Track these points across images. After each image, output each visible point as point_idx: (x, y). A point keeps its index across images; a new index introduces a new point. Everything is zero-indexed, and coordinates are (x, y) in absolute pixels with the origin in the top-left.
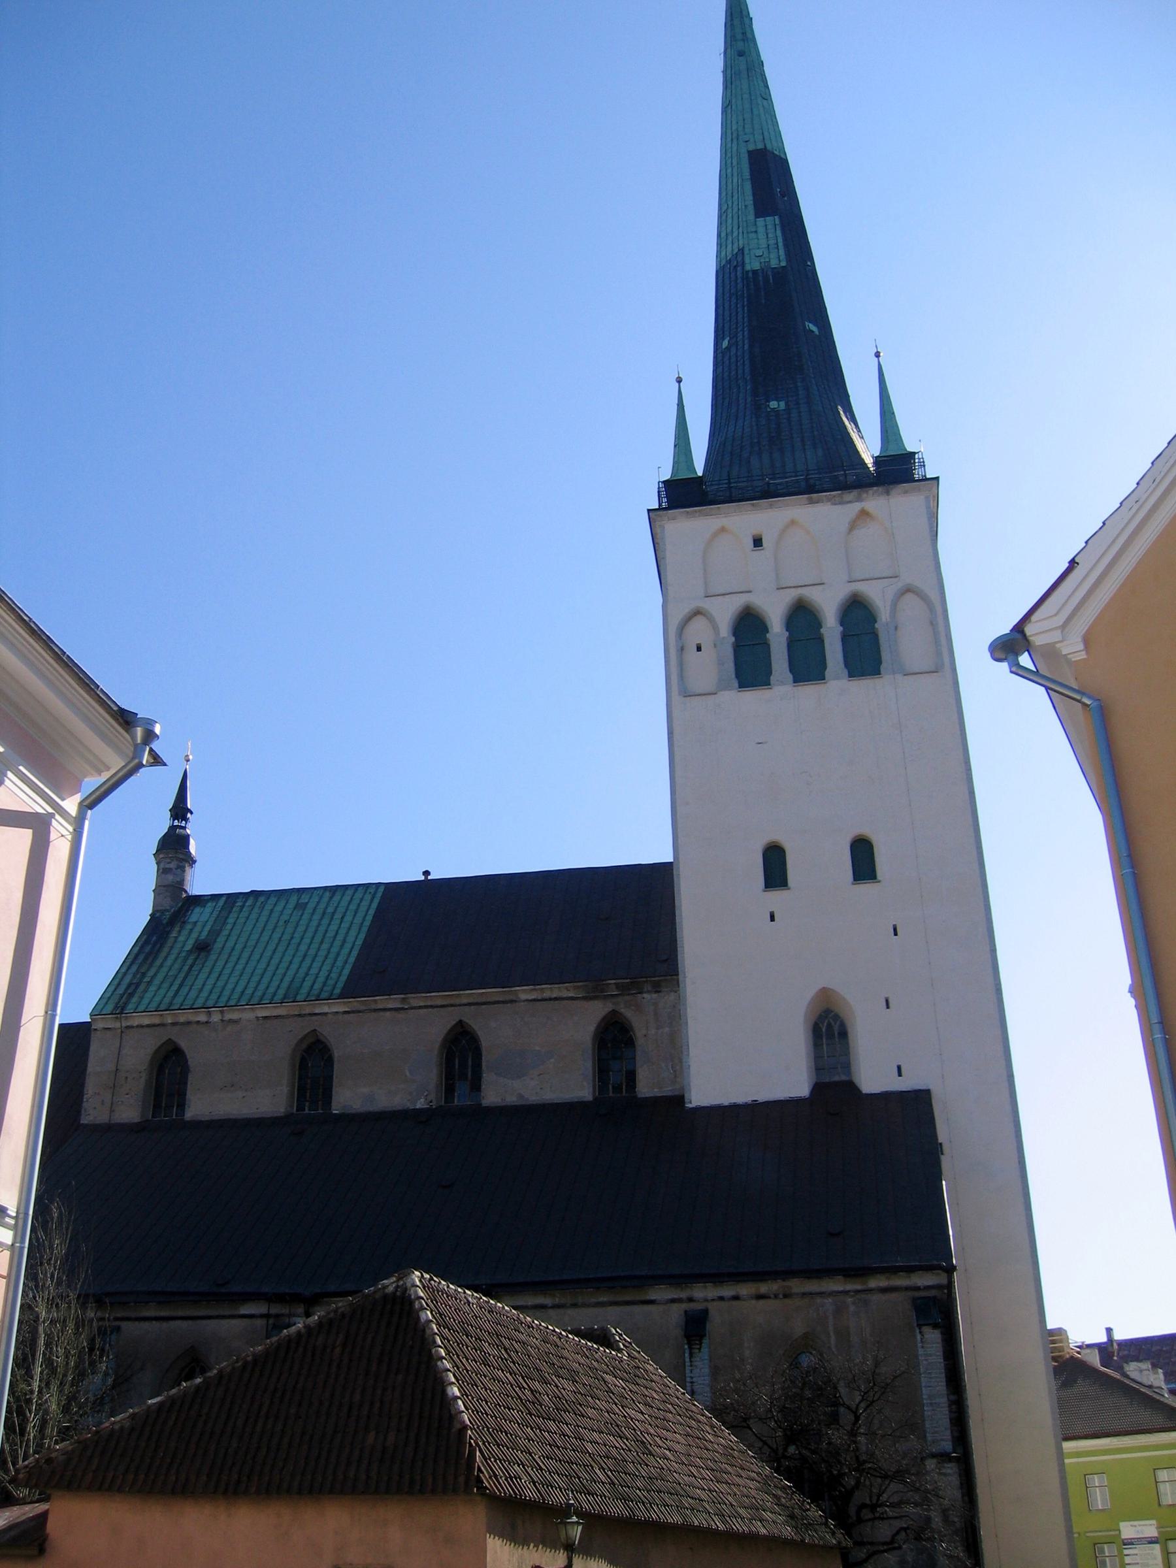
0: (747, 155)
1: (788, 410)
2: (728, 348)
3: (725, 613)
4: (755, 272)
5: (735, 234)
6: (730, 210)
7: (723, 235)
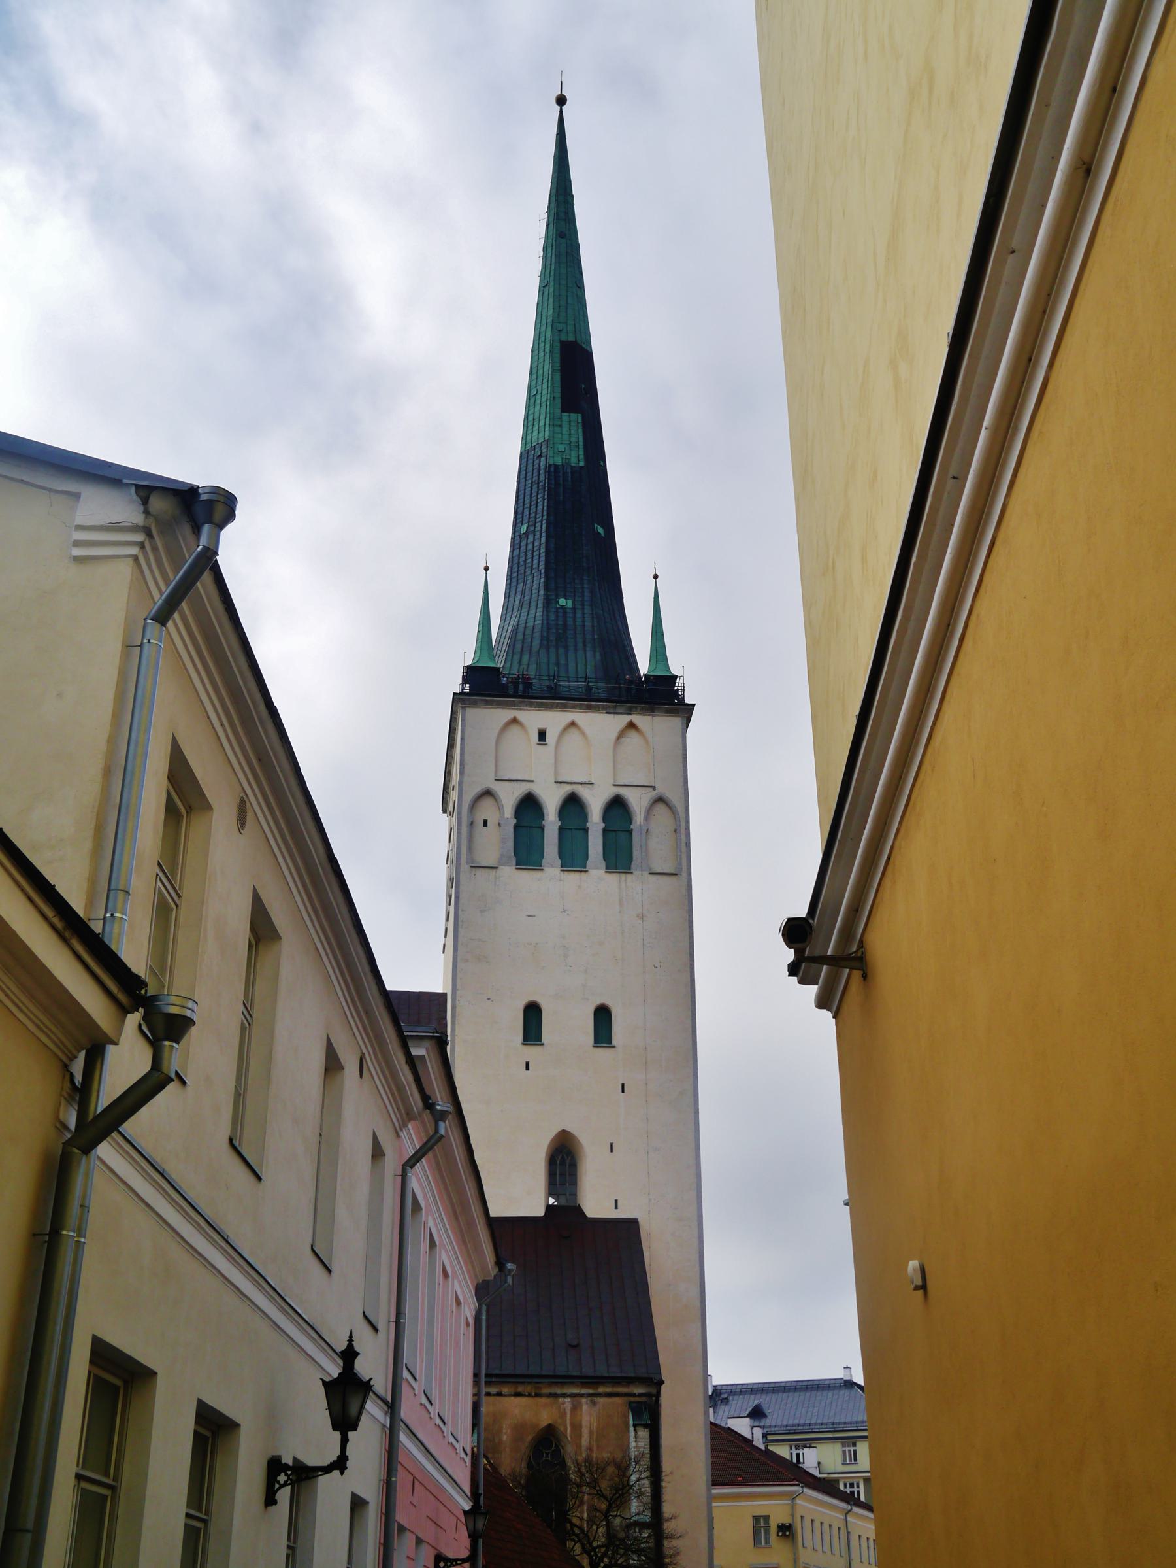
0: (558, 344)
1: (574, 609)
2: (526, 534)
3: (510, 797)
4: (556, 467)
5: (542, 423)
6: (538, 396)
7: (531, 418)
